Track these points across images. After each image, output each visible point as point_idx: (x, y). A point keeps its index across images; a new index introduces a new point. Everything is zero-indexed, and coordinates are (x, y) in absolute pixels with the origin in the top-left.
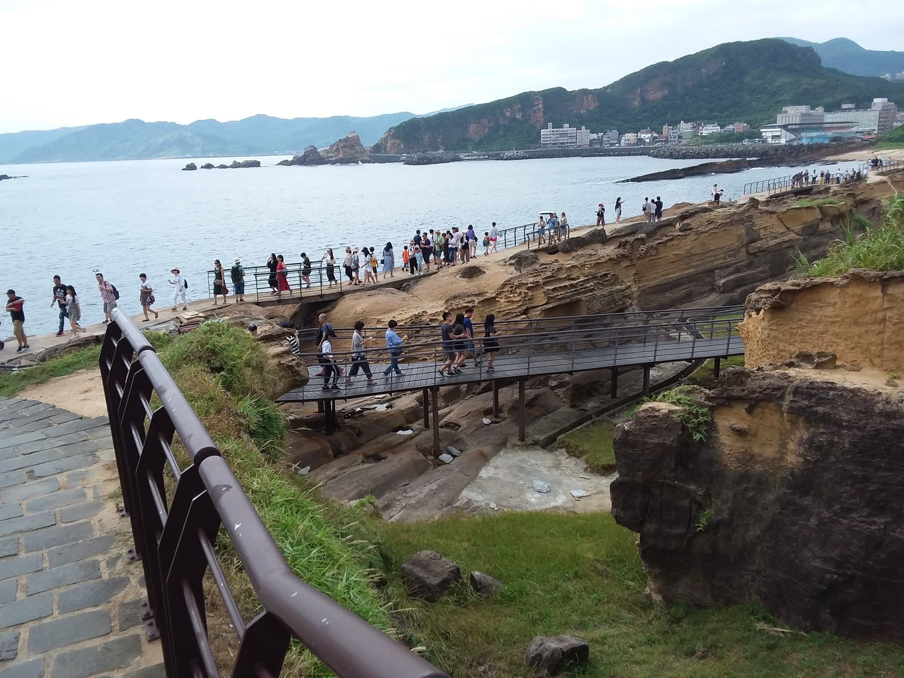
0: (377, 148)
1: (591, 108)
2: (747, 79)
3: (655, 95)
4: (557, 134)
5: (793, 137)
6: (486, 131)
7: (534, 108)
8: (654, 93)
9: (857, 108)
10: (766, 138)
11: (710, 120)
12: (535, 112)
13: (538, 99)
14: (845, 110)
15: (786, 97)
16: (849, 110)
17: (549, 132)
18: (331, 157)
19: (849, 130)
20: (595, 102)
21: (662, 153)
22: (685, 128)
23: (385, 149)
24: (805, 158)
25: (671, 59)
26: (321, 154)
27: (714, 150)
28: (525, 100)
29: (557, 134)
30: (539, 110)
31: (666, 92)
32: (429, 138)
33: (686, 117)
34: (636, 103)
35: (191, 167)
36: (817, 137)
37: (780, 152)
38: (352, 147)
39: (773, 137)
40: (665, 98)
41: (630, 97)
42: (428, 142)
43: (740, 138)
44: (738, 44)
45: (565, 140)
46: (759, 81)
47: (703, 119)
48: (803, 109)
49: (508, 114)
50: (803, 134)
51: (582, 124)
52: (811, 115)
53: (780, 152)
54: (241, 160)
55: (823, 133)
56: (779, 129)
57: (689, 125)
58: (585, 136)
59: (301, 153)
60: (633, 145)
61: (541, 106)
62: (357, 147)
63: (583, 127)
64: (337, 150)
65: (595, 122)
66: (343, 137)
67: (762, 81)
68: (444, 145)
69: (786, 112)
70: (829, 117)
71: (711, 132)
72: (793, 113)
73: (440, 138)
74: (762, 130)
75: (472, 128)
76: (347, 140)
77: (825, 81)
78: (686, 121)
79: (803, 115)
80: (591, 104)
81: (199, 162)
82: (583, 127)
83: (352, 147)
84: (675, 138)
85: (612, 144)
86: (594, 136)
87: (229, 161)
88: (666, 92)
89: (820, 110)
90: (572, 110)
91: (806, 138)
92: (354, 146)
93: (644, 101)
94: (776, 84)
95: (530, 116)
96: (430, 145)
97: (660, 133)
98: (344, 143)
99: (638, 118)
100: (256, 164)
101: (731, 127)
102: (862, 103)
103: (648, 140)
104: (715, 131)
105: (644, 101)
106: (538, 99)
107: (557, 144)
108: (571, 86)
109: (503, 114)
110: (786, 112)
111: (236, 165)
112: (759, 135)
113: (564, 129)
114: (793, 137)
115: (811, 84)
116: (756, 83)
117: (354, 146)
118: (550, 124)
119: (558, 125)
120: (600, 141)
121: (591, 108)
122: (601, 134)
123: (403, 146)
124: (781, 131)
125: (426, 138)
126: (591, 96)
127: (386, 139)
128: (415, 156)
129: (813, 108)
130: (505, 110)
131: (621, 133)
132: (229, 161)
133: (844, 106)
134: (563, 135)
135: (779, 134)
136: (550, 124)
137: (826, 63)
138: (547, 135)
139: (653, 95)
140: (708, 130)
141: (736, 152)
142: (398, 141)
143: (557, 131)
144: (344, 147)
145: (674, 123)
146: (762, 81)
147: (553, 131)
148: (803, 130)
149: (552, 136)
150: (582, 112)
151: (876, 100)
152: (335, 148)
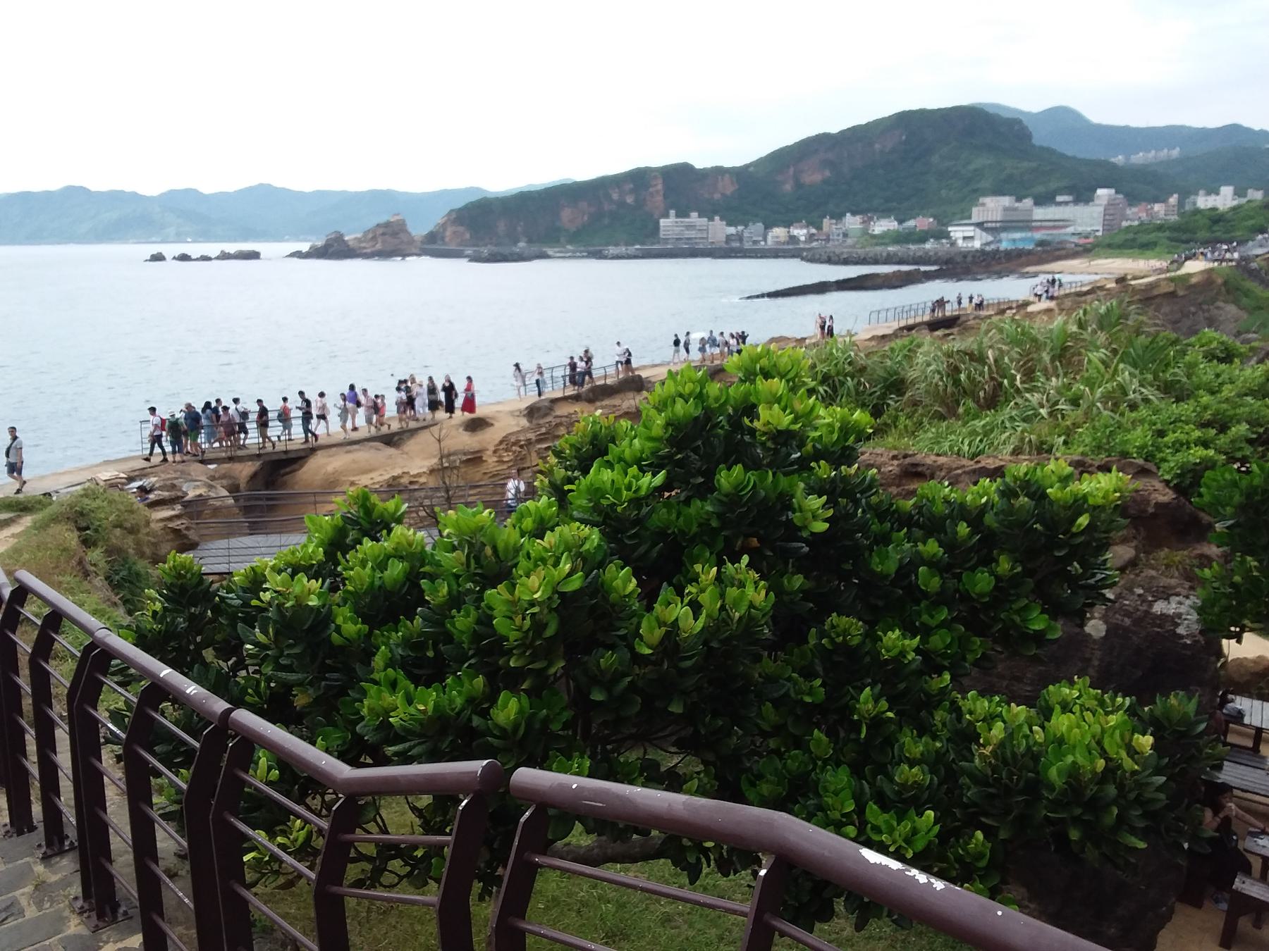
0: (432, 237)
1: (728, 193)
2: (935, 159)
3: (813, 177)
5: (990, 238)
6: (586, 218)
7: (651, 190)
9: (1077, 201)
11: (885, 213)
12: (652, 195)
13: (655, 178)
14: (1060, 204)
15: (985, 184)
16: (1066, 203)
18: (365, 248)
19: (1063, 231)
21: (817, 256)
22: (852, 222)
23: (443, 239)
24: (998, 268)
25: (834, 130)
26: (350, 243)
27: (885, 254)
28: (639, 178)
30: (657, 192)
31: (827, 173)
33: (854, 208)
34: (788, 187)
35: (158, 258)
36: (1022, 240)
37: (969, 259)
38: (395, 234)
39: (965, 238)
40: (825, 182)
41: (779, 178)
43: (922, 238)
44: (922, 113)
45: (692, 234)
47: (875, 210)
48: (1006, 201)
49: (615, 196)
50: (1003, 235)
51: (715, 212)
52: (1015, 209)
53: (969, 259)
54: (232, 248)
55: (1029, 234)
57: (858, 218)
58: (720, 230)
59: (320, 243)
60: (784, 243)
61: (660, 187)
63: (717, 218)
64: (374, 238)
65: (734, 211)
66: (383, 219)
69: (983, 205)
70: (1040, 213)
71: (885, 229)
72: (993, 207)
74: (950, 229)
75: (566, 214)
76: (388, 225)
77: (1034, 164)
78: (854, 213)
79: (1006, 209)
81: (171, 250)
82: (717, 218)
83: (395, 234)
84: (838, 235)
85: (755, 242)
86: (732, 230)
87: (213, 249)
88: (827, 173)
89: (1028, 202)
91: (1007, 242)
92: (397, 234)
93: (798, 185)
94: (972, 167)
97: (819, 228)
100: (254, 255)
101: (911, 223)
102: (1083, 195)
103: (803, 238)
104: (892, 228)
105: (798, 185)
106: (655, 178)
107: (681, 239)
110: (983, 205)
111: (225, 256)
112: (947, 235)
114: (990, 238)
118: (672, 212)
119: (683, 213)
120: (740, 237)
121: (728, 193)
122: (740, 228)
125: (502, 226)
127: (444, 226)
128: (485, 251)
129: (1019, 199)
131: (768, 227)
132: (213, 249)
133: (1059, 199)
134: (690, 227)
135: (971, 234)
136: (672, 212)
137: (1039, 139)
140: (882, 226)
141: (913, 258)
142: (461, 229)
144: (383, 234)
145: (838, 216)
148: (1005, 229)
150: (717, 196)
151: (1100, 192)
152: (370, 236)
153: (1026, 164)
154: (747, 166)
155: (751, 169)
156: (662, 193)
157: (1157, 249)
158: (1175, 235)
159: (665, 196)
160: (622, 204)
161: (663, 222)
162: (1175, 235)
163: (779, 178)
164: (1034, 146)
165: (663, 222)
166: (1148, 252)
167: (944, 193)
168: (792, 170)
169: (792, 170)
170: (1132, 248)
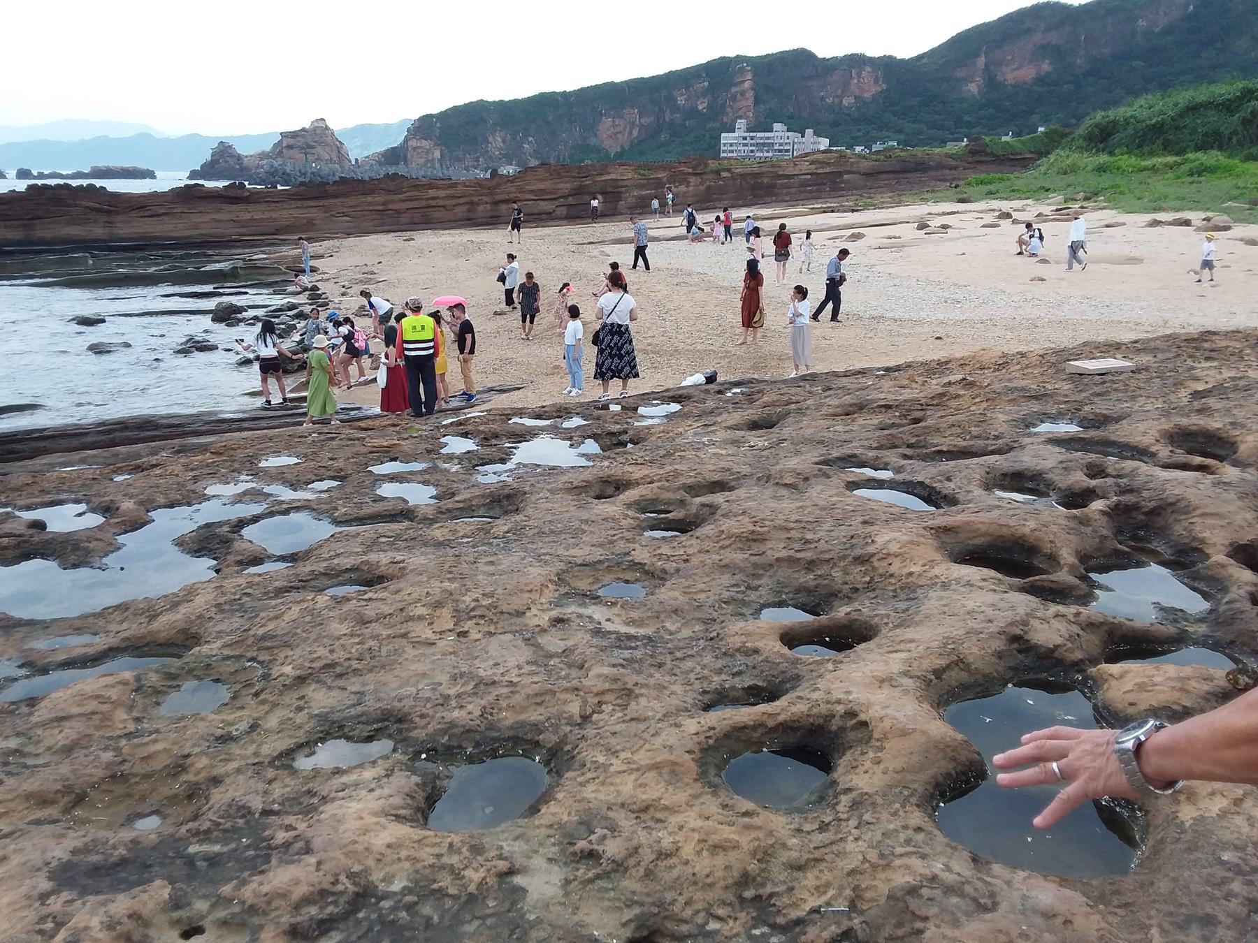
4: (752, 145)
6: (635, 133)
7: (734, 90)
8: (1017, 69)
12: (734, 99)
17: (736, 138)
20: (876, 81)
29: (752, 145)
30: (743, 93)
31: (1046, 67)
32: (504, 142)
34: (973, 88)
40: (1040, 80)
41: (961, 73)
42: (500, 149)
49: (681, 101)
61: (747, 85)
62: (319, 150)
63: (809, 132)
68: (537, 158)
73: (529, 143)
80: (869, 87)
82: (809, 132)
90: (822, 98)
92: (313, 147)
93: (992, 83)
95: (724, 105)
96: (505, 156)
98: (292, 141)
99: (966, 118)
108: (825, 50)
109: (671, 100)
113: (767, 134)
117: (313, 147)
123: (437, 154)
126: (868, 69)
127: (406, 140)
130: (676, 93)
136: (741, 123)
138: (731, 145)
139: (1017, 73)
142: (426, 144)
143: (752, 138)
147: (745, 138)
149: (741, 148)
150: (846, 102)
154: (920, 57)
155: (925, 60)
156: (750, 94)
159: (757, 101)
160: (692, 112)
161: (726, 137)
163: (961, 73)
165: (726, 137)
168: (981, 61)
169: (981, 61)
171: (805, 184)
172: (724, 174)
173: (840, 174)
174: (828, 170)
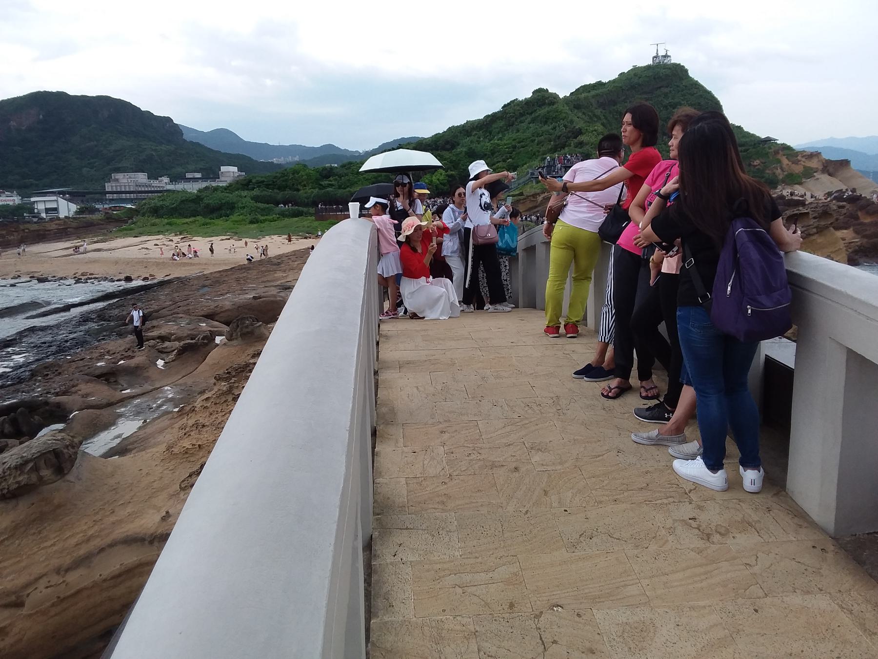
10: (39, 213)
39: (47, 210)
46: (92, 143)
48: (142, 177)
56: (54, 198)
67: (95, 143)
74: (33, 199)
104: (11, 203)
110: (117, 180)
115: (155, 150)
116: (88, 144)
124: (57, 201)
133: (189, 175)
135: (54, 205)
146: (95, 143)
153: (164, 147)
157: (234, 217)
158: (268, 192)
162: (268, 192)
164: (185, 141)
166: (219, 222)
167: (85, 170)
170: (194, 214)
171: (55, 233)
172: (27, 231)
173: (67, 228)
174: (62, 227)
